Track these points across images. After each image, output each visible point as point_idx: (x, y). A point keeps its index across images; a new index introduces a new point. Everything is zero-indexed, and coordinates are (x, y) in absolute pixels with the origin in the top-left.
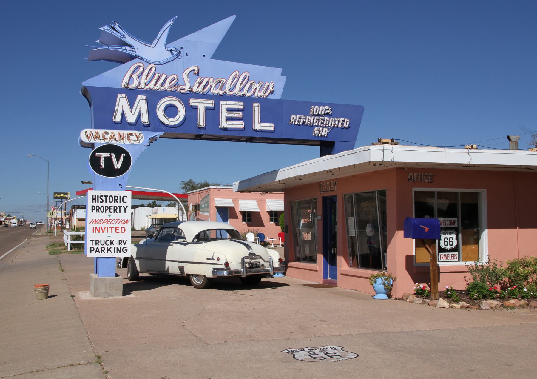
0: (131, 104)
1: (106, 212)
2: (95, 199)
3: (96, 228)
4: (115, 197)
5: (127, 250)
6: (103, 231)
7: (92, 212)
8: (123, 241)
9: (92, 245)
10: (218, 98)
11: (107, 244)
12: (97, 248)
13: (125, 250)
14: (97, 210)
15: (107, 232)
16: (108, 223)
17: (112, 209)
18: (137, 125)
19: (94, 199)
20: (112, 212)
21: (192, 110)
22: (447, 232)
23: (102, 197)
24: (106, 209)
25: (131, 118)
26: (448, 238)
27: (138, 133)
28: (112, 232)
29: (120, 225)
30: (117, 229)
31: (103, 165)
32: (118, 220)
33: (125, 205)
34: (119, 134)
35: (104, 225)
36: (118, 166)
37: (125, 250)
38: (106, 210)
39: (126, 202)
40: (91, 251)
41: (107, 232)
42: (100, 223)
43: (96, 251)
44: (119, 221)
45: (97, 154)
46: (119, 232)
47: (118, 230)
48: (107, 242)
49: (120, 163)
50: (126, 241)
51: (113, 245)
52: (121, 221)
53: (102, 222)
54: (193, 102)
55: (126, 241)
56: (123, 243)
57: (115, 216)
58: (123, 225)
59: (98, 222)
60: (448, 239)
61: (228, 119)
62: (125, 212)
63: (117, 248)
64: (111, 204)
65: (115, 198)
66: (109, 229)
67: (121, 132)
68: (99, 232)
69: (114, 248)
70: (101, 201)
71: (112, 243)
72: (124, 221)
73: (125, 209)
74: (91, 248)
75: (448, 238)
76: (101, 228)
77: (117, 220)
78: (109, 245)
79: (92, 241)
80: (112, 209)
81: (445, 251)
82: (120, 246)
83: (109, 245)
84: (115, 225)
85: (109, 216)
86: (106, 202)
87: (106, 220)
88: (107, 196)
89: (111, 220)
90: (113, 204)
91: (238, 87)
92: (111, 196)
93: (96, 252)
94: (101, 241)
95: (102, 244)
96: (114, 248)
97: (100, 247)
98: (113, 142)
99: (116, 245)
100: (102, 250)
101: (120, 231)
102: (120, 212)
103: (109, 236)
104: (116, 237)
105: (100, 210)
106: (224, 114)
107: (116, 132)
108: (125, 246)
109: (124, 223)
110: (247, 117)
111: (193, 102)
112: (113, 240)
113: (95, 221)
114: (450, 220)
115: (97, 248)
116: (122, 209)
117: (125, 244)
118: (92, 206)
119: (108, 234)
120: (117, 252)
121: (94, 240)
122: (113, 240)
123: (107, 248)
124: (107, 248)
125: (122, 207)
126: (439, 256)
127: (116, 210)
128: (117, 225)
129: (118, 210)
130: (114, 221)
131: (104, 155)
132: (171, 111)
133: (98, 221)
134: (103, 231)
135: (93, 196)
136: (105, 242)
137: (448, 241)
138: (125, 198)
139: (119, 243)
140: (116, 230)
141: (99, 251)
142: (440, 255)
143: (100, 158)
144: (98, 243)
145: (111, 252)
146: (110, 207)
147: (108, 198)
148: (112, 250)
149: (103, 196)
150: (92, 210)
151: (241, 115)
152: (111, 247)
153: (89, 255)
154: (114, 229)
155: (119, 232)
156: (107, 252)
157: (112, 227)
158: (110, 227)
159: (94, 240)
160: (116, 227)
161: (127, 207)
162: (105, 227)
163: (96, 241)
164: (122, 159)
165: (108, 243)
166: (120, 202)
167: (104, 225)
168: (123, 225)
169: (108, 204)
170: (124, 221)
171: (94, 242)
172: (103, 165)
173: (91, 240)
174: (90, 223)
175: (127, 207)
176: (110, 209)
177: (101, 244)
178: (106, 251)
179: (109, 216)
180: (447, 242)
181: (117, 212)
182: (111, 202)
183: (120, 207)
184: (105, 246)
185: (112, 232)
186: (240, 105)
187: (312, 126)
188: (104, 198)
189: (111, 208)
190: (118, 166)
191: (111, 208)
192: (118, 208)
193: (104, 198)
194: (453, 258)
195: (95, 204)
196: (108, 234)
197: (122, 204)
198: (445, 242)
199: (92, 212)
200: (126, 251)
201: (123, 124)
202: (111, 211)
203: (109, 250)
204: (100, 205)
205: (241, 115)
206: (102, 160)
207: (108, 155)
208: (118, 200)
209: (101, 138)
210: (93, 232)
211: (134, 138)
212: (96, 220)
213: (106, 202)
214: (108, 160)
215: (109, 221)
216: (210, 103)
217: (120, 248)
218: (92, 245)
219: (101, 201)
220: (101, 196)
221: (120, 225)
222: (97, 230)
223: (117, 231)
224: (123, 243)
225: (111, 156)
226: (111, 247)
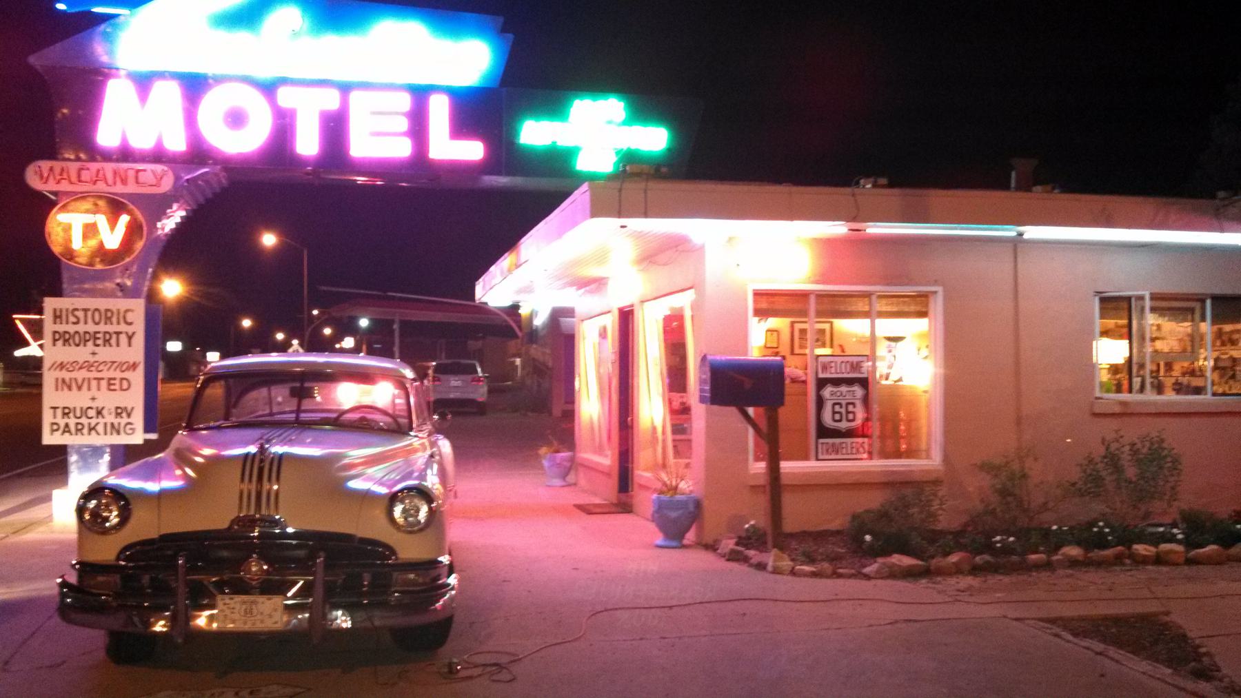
1: (85, 345)
2: (60, 317)
3: (63, 381)
4: (107, 310)
5: (133, 429)
6: (79, 388)
7: (54, 345)
8: (126, 408)
9: (55, 417)
11: (90, 416)
12: (67, 425)
13: (131, 429)
15: (89, 389)
16: (92, 369)
17: (99, 338)
19: (57, 317)
20: (98, 345)
22: (838, 389)
23: (77, 313)
24: (85, 338)
26: (844, 402)
28: (99, 389)
29: (118, 375)
30: (112, 382)
32: (114, 362)
33: (130, 329)
34: (115, 173)
35: (81, 375)
37: (131, 429)
39: (130, 324)
40: (53, 431)
41: (89, 389)
42: (71, 369)
43: (64, 432)
44: (116, 365)
46: (115, 390)
47: (114, 384)
48: (90, 410)
50: (133, 408)
51: (103, 417)
52: (121, 364)
53: (77, 367)
54: (286, 97)
55: (133, 408)
56: (124, 415)
57: (105, 353)
58: (125, 375)
59: (68, 368)
60: (841, 407)
62: (130, 345)
63: (112, 424)
64: (97, 328)
65: (106, 314)
66: (94, 383)
68: (70, 388)
69: (105, 424)
70: (74, 320)
71: (99, 413)
72: (126, 365)
73: (130, 338)
74: (53, 424)
75: (844, 402)
76: (76, 379)
77: (111, 362)
78: (91, 418)
79: (55, 408)
80: (99, 338)
81: (836, 433)
82: (119, 420)
83: (91, 418)
84: (105, 374)
86: (86, 323)
87: (86, 364)
88: (89, 310)
89: (97, 362)
90: (102, 328)
92: (96, 310)
93: (63, 434)
94: (75, 408)
95: (78, 415)
96: (105, 424)
97: (72, 422)
99: (110, 418)
100: (78, 430)
101: (117, 387)
102: (118, 345)
103: (93, 399)
105: (71, 341)
108: (130, 420)
109: (128, 369)
112: (103, 408)
113: (62, 366)
114: (848, 362)
115: (67, 425)
116: (123, 338)
117: (129, 415)
118: (55, 332)
119: (90, 394)
120: (112, 434)
121: (58, 408)
122: (103, 408)
123: (89, 424)
124: (89, 424)
125: (121, 333)
126: (820, 446)
127: (108, 341)
128: (111, 374)
129: (113, 341)
130: (105, 365)
133: (68, 366)
134: (79, 388)
135: (55, 310)
136: (84, 412)
137: (843, 410)
140: (110, 384)
141: (69, 432)
142: (822, 443)
144: (67, 414)
145: (98, 434)
147: (89, 314)
148: (100, 428)
149: (76, 310)
150: (55, 340)
152: (97, 424)
153: (49, 439)
154: (104, 383)
155: (115, 390)
156: (89, 434)
157: (99, 379)
158: (95, 379)
159: (58, 408)
160: (110, 379)
161: (134, 333)
162: (84, 379)
163: (64, 408)
165: (92, 413)
166: (118, 323)
167: (81, 375)
168: (126, 375)
169: (91, 328)
170: (126, 365)
171: (59, 412)
173: (52, 408)
174: (50, 369)
175: (134, 333)
178: (85, 431)
179: (94, 354)
180: (840, 413)
181: (111, 346)
182: (97, 324)
183: (118, 333)
184: (84, 420)
185: (99, 389)
188: (80, 314)
189: (98, 335)
191: (98, 335)
192: (114, 336)
193: (80, 314)
194: (854, 451)
195: (61, 328)
196: (90, 394)
197: (123, 327)
198: (834, 413)
199: (54, 345)
200: (131, 432)
202: (99, 342)
203: (94, 428)
204: (71, 329)
208: (114, 320)
209: (74, 178)
210: (57, 390)
212: (62, 363)
213: (86, 323)
215: (92, 366)
216: (330, 100)
217: (119, 424)
218: (55, 417)
219: (74, 320)
221: (118, 375)
222: (66, 385)
223: (112, 387)
224: (124, 415)
226: (97, 424)
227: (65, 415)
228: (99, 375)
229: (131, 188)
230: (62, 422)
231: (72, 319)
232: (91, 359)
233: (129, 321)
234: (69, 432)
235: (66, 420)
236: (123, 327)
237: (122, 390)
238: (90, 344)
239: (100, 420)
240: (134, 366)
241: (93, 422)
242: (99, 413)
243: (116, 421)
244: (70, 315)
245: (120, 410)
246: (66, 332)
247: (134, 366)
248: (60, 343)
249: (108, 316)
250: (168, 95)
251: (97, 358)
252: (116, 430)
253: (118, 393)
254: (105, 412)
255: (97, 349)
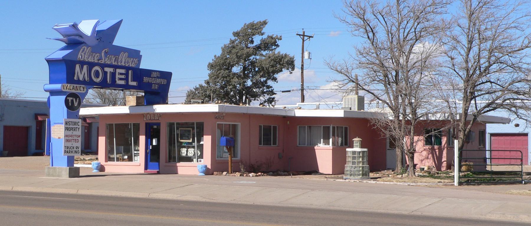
0: (82, 69)
4: (75, 122)
5: (79, 152)
6: (70, 142)
10: (116, 67)
12: (67, 151)
14: (68, 129)
15: (72, 142)
18: (84, 82)
21: (105, 73)
25: (81, 79)
27: (84, 86)
32: (76, 135)
35: (70, 138)
38: (71, 130)
45: (68, 98)
49: (77, 102)
54: (106, 69)
57: (75, 133)
61: (121, 79)
66: (72, 140)
67: (77, 85)
71: (73, 148)
73: (79, 129)
79: (65, 147)
84: (74, 138)
85: (72, 133)
90: (74, 126)
91: (123, 61)
97: (68, 150)
98: (74, 91)
99: (75, 149)
100: (69, 152)
101: (76, 141)
103: (72, 144)
104: (75, 145)
106: (117, 76)
107: (75, 85)
109: (78, 137)
110: (126, 79)
111: (106, 69)
115: (67, 151)
117: (78, 148)
129: (76, 130)
131: (70, 99)
132: (97, 74)
134: (70, 142)
138: (79, 123)
139: (76, 148)
140: (75, 141)
141: (68, 153)
143: (69, 100)
146: (73, 128)
151: (123, 77)
154: (74, 140)
157: (73, 139)
160: (75, 139)
164: (78, 101)
165: (72, 148)
167: (70, 138)
169: (72, 126)
171: (66, 147)
176: (73, 129)
177: (69, 149)
178: (71, 152)
183: (77, 128)
184: (70, 150)
186: (123, 71)
187: (152, 84)
188: (70, 123)
193: (70, 123)
197: (78, 126)
201: (78, 82)
204: (69, 126)
205: (123, 77)
206: (70, 100)
207: (72, 98)
211: (82, 89)
214: (72, 101)
220: (69, 122)
221: (77, 138)
225: (73, 99)
227: (67, 148)
228: (73, 138)
229: (79, 91)
230: (67, 150)
231: (69, 124)
232: (72, 134)
233: (79, 124)
234: (68, 153)
235: (67, 150)
236: (78, 126)
237: (77, 142)
238: (72, 130)
239: (74, 150)
240: (79, 136)
241: (72, 150)
242: (73, 148)
243: (76, 150)
244: (70, 124)
245: (77, 148)
246: (68, 127)
247: (79, 136)
248: (67, 130)
249: (75, 123)
250: (85, 67)
251: (74, 134)
253: (76, 143)
254: (74, 148)
255: (73, 132)
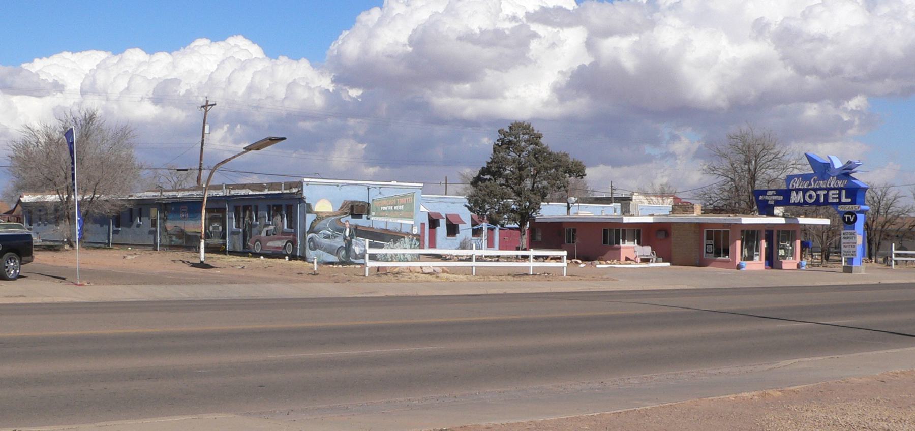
19: (844, 234)
31: (847, 220)
35: (847, 245)
36: (852, 220)
57: (851, 241)
90: (850, 236)
98: (849, 210)
131: (847, 216)
136: (848, 252)
143: (845, 217)
167: (847, 245)
169: (849, 236)
172: (847, 220)
190: (852, 220)
214: (849, 218)
222: (845, 246)
252: (853, 255)
